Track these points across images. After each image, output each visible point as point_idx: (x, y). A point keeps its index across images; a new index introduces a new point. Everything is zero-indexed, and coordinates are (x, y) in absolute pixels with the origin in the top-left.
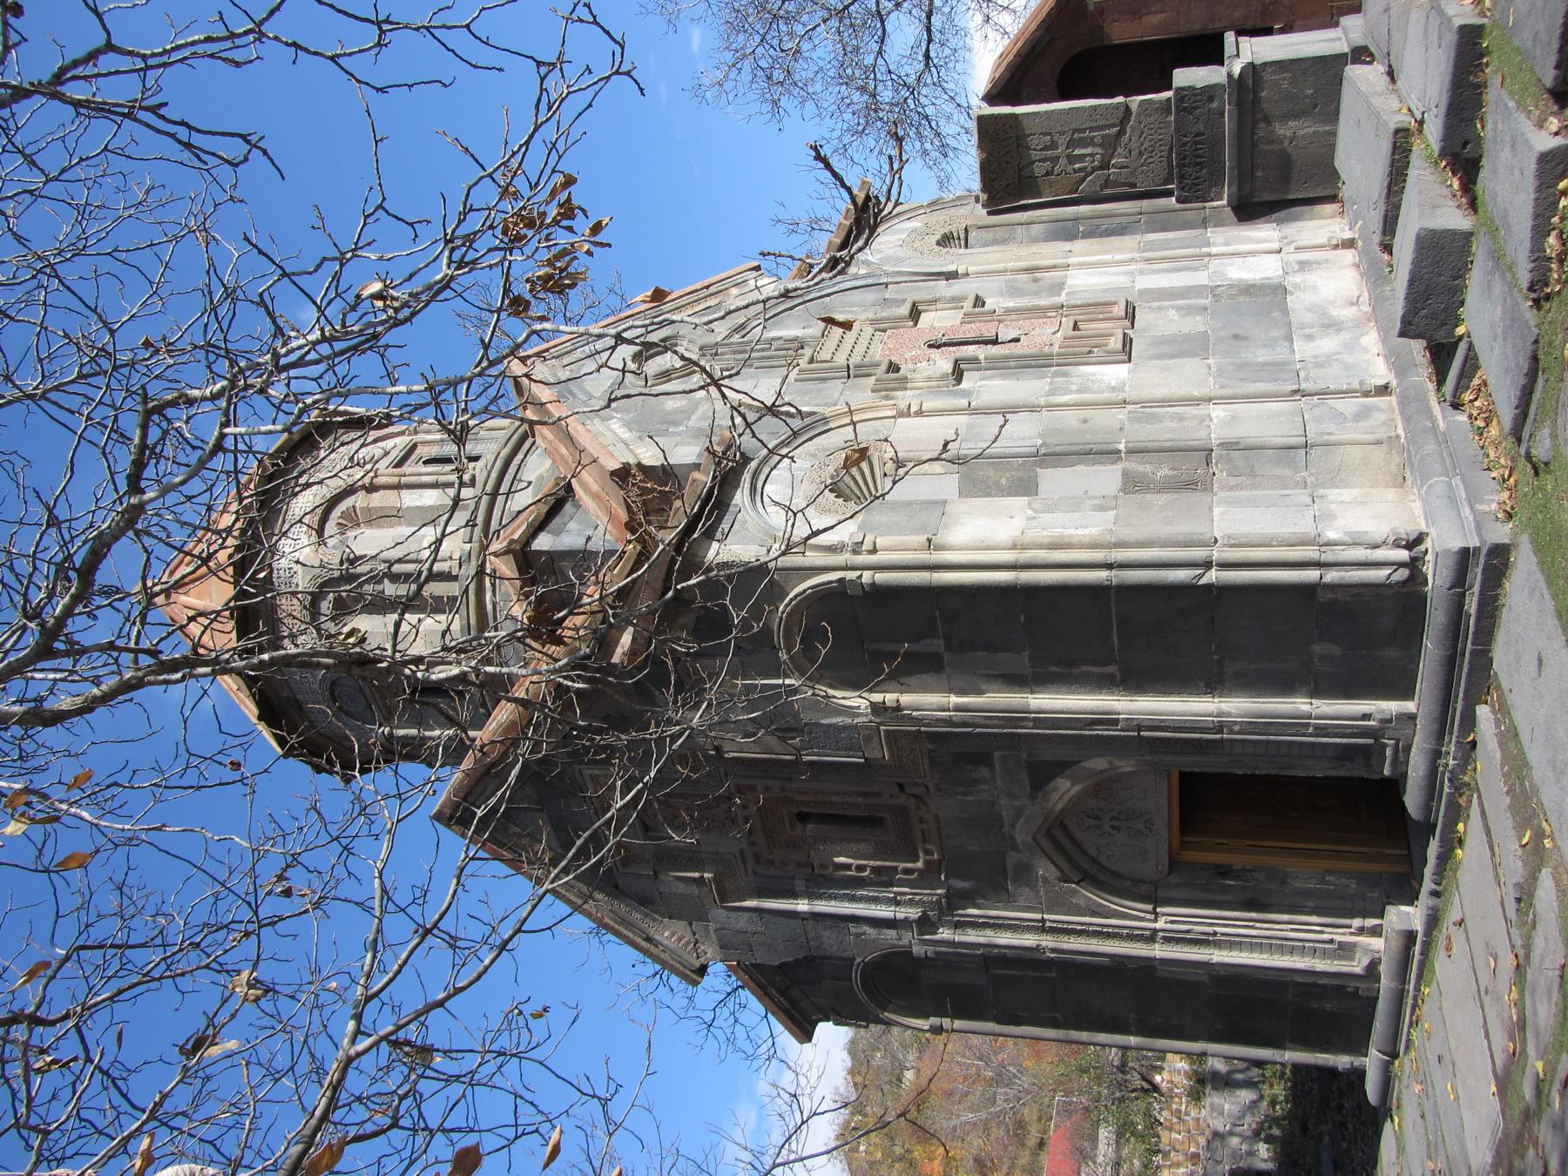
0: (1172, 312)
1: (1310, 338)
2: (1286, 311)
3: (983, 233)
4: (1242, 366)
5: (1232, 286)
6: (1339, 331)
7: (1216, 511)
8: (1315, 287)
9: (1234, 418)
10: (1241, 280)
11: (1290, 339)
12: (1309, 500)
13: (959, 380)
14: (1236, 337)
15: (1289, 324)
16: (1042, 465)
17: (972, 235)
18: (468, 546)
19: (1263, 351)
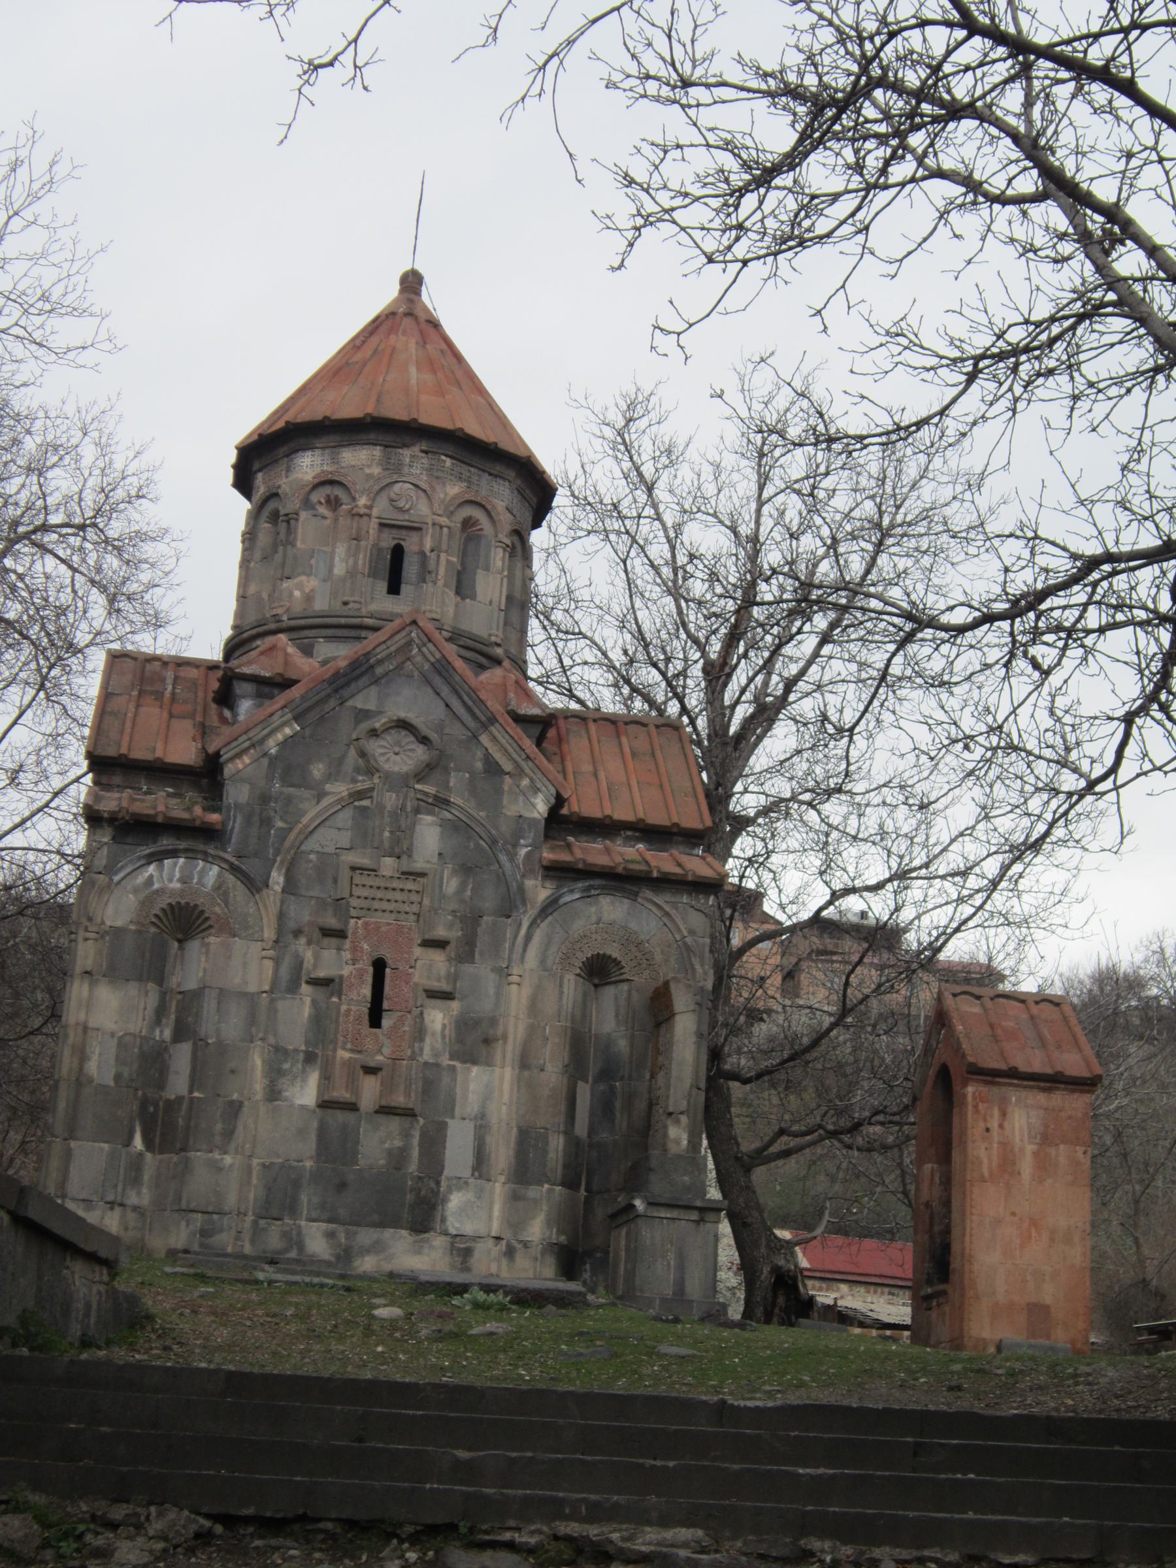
0: (398, 1143)
1: (330, 1235)
2: (382, 1225)
3: (625, 995)
4: (296, 1184)
5: (437, 1193)
6: (338, 1257)
7: (106, 1146)
8: (419, 1252)
9: (220, 1170)
10: (445, 1201)
11: (329, 1221)
12: (110, 1198)
13: (308, 982)
14: (342, 1186)
15: (358, 1225)
16: (195, 1045)
17: (625, 987)
18: (285, 618)
19: (315, 1200)
